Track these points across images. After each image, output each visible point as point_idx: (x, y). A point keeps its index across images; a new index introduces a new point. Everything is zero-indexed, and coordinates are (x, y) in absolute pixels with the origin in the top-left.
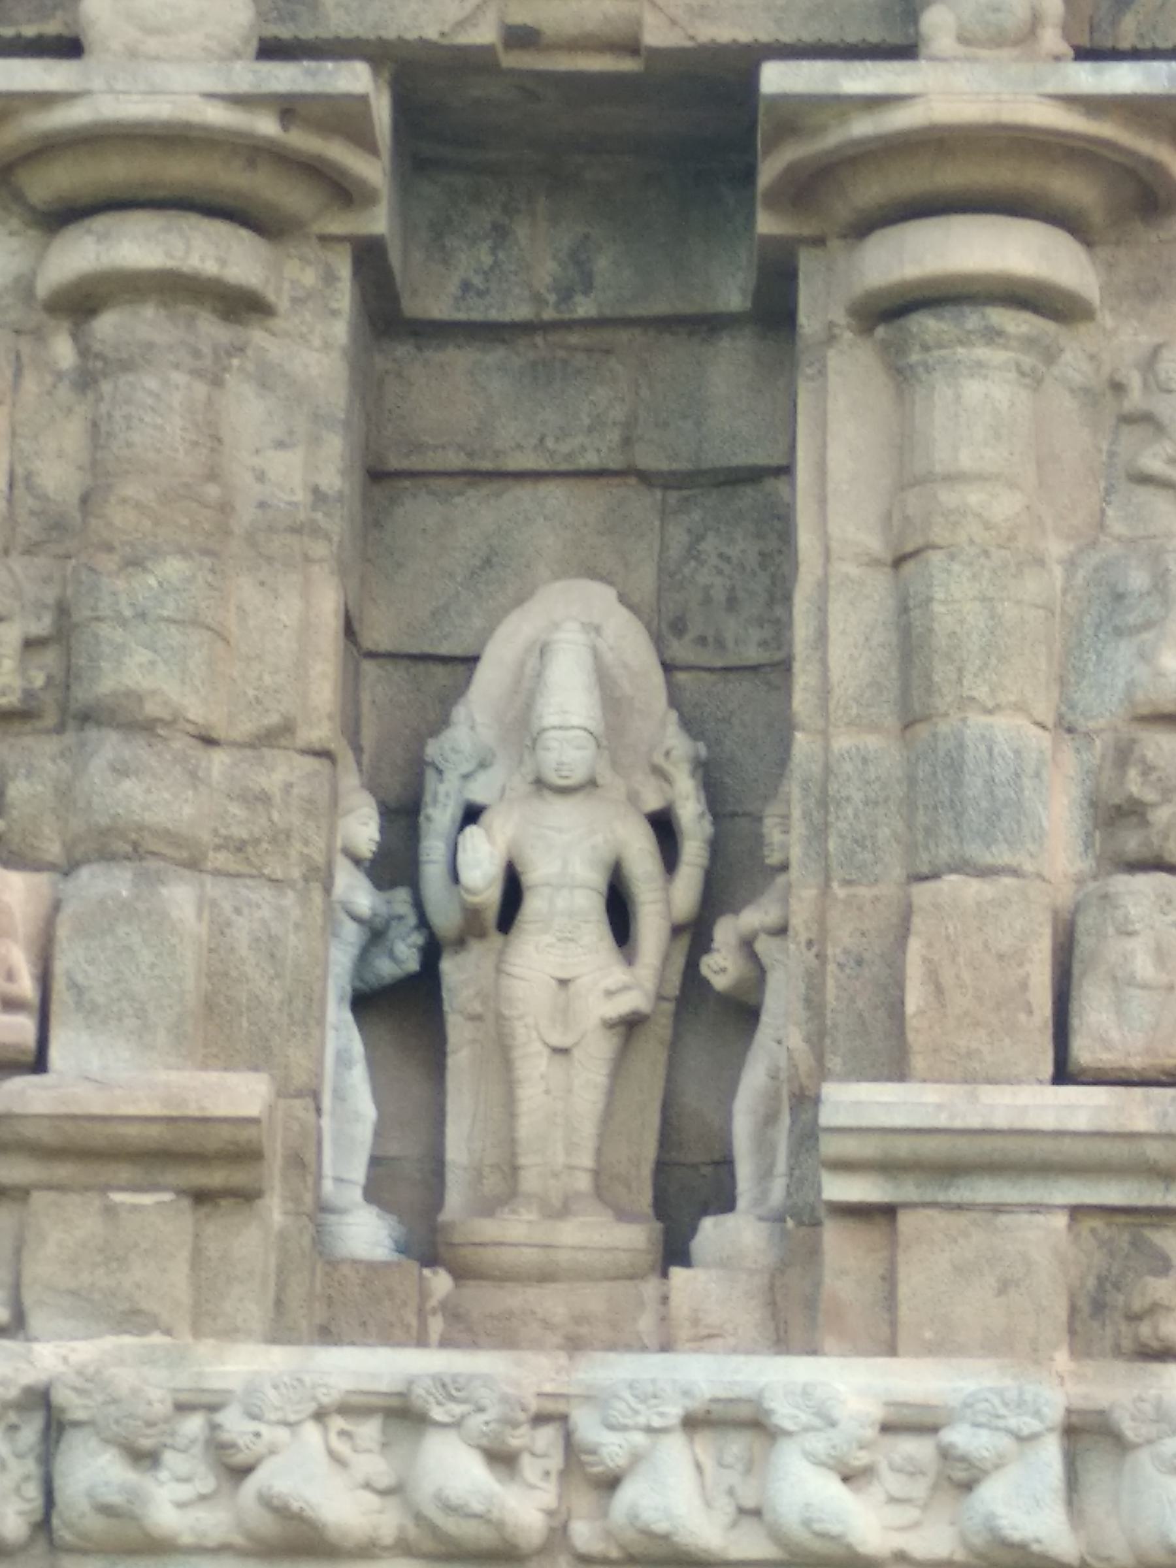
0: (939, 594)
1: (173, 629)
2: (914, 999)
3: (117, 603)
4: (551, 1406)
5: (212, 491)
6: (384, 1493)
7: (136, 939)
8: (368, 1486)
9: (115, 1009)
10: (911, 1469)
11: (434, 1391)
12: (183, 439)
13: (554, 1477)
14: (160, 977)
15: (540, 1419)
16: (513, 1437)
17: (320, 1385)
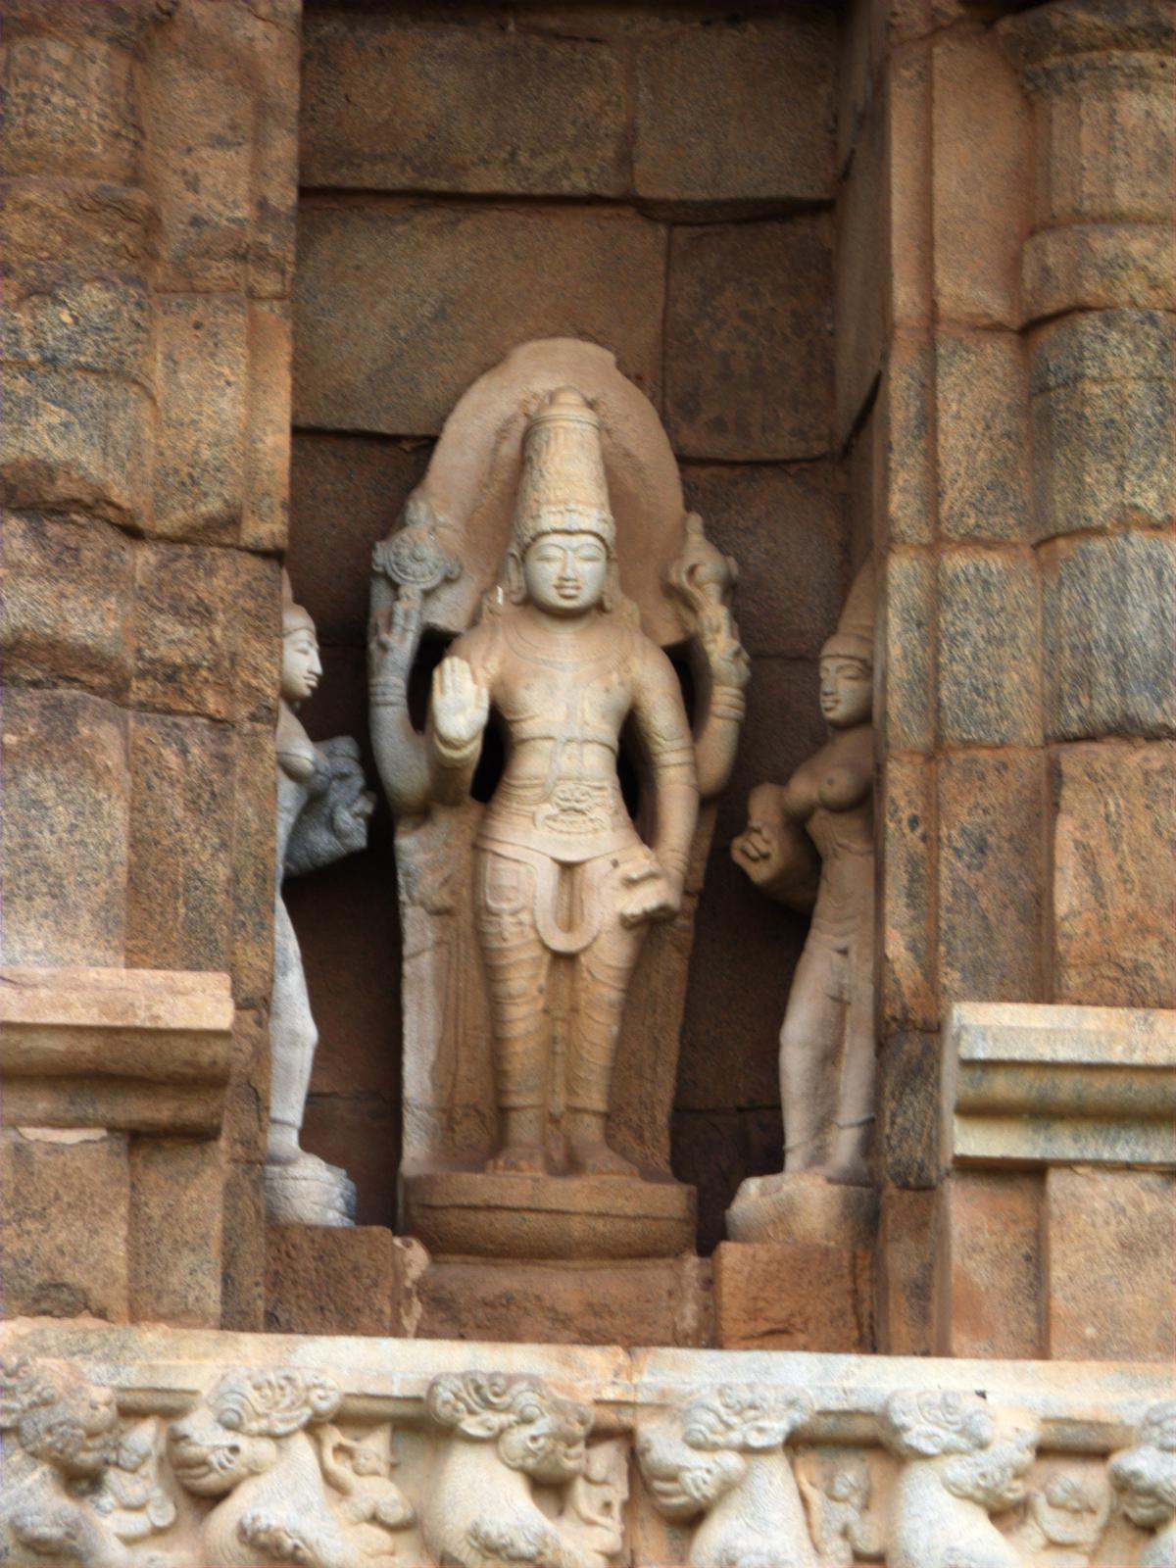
0: (1092, 371)
1: (92, 379)
2: (1068, 896)
3: (18, 343)
4: (610, 1417)
5: (139, 197)
6: (394, 1529)
7: (48, 793)
8: (374, 1519)
9: (22, 883)
10: (1076, 1504)
11: (464, 1395)
12: (101, 128)
13: (616, 1510)
14: (82, 843)
15: (598, 1435)
16: (566, 1456)
17: (315, 1386)
